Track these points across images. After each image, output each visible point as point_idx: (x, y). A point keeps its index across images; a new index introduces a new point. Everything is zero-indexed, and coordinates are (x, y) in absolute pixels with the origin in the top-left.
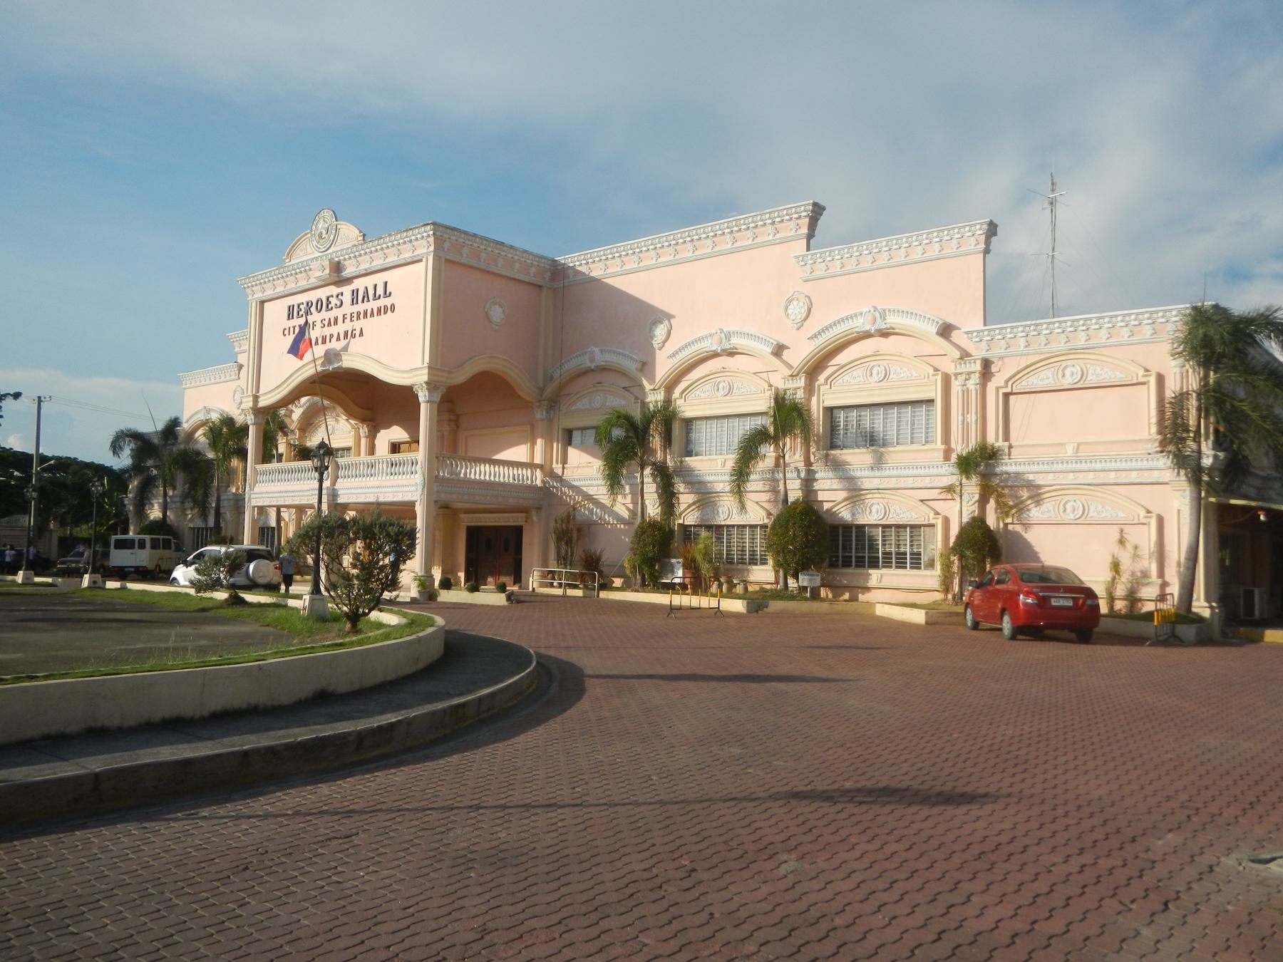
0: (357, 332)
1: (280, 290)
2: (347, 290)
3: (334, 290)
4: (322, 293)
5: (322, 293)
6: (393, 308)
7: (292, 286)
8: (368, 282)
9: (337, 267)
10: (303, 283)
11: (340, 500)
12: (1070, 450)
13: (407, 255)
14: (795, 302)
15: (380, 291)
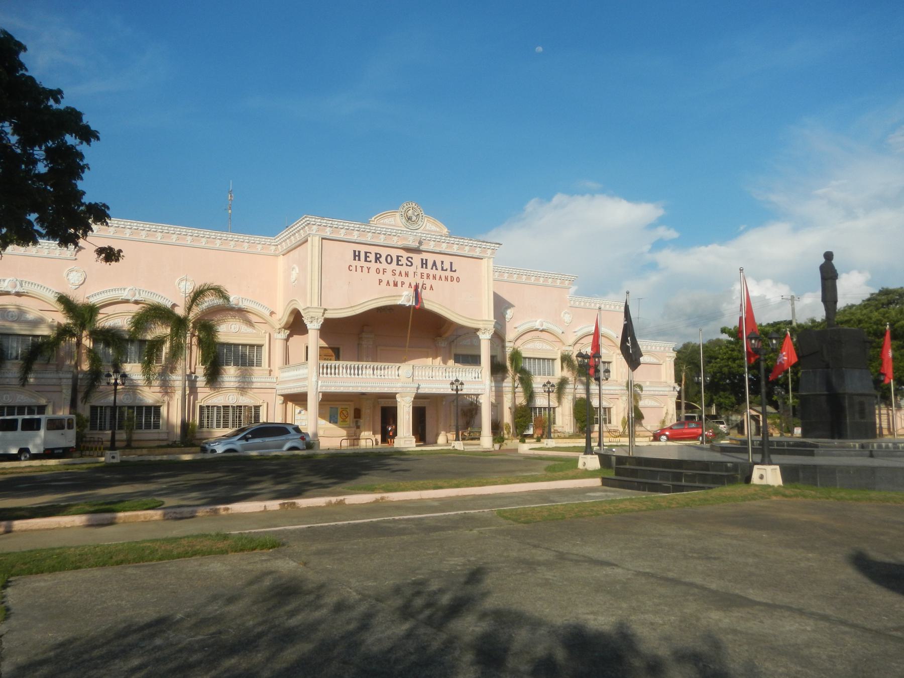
0: (428, 287)
1: (355, 236)
2: (417, 258)
3: (405, 255)
4: (395, 253)
5: (395, 253)
6: (458, 280)
7: (369, 238)
8: (438, 258)
9: (420, 243)
10: (381, 240)
11: (420, 391)
12: (648, 383)
13: (477, 252)
14: (567, 315)
15: (447, 266)
